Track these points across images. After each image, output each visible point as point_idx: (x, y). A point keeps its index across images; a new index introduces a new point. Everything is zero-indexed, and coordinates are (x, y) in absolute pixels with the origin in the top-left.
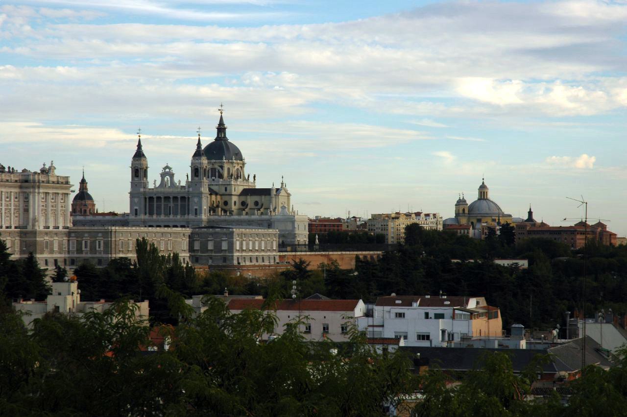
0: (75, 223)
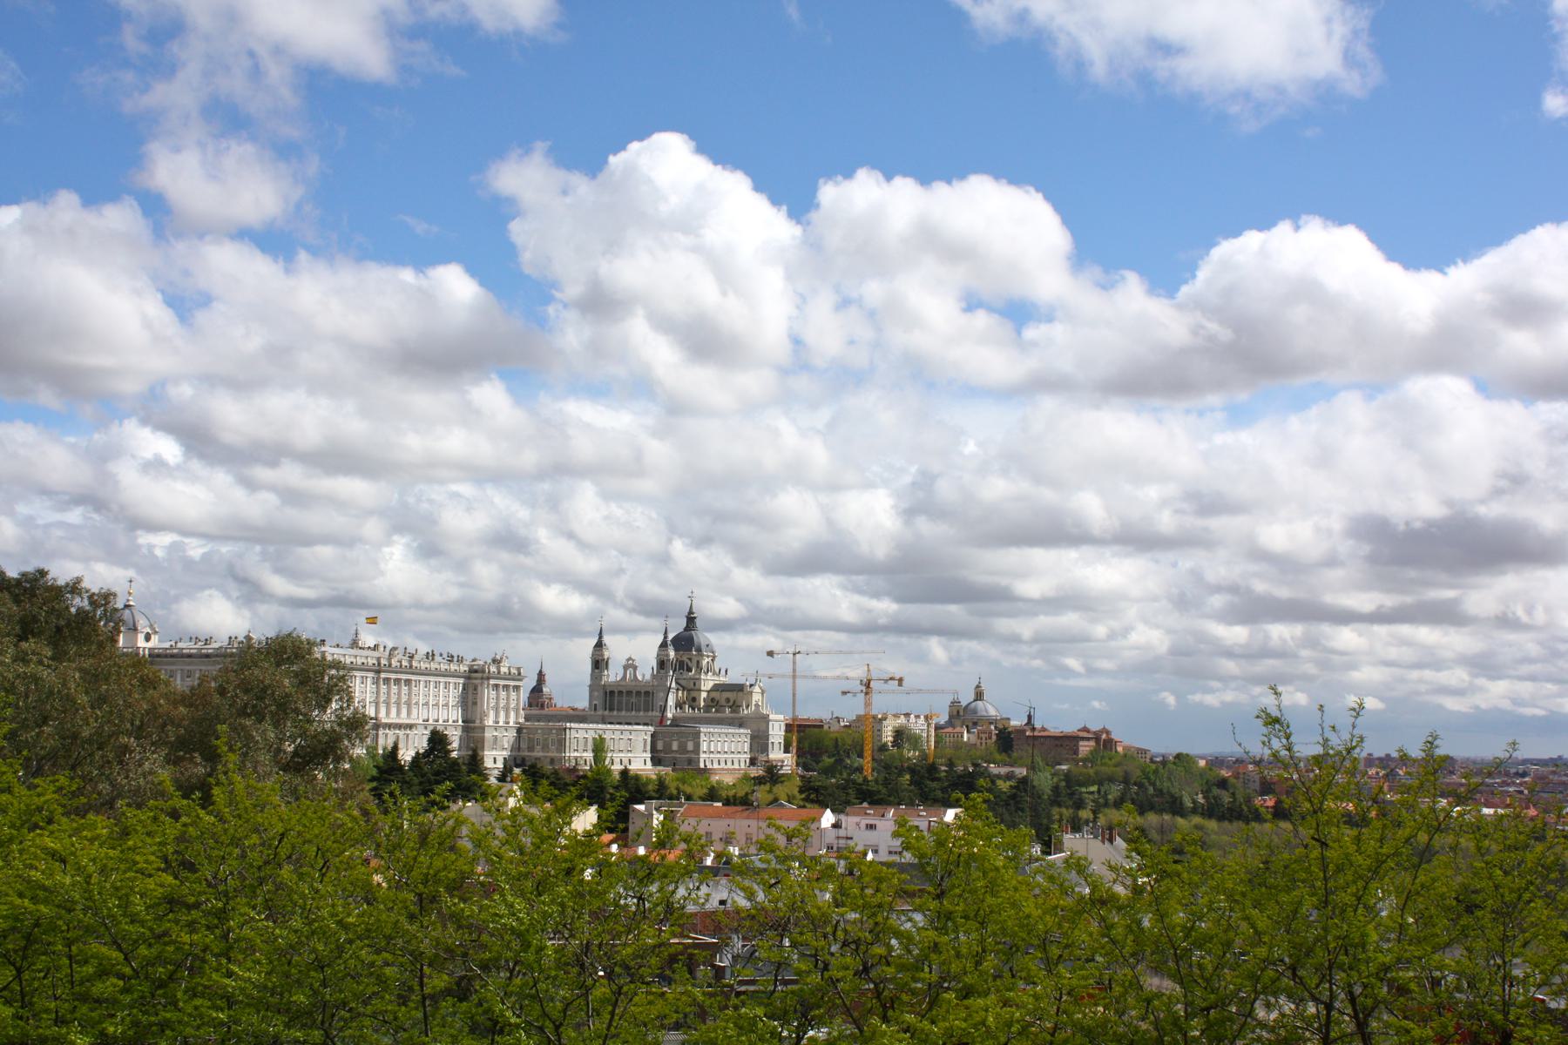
0: (527, 719)
